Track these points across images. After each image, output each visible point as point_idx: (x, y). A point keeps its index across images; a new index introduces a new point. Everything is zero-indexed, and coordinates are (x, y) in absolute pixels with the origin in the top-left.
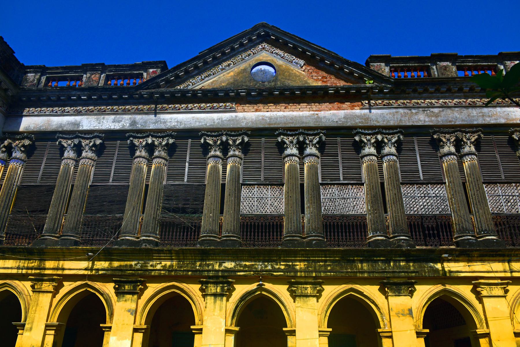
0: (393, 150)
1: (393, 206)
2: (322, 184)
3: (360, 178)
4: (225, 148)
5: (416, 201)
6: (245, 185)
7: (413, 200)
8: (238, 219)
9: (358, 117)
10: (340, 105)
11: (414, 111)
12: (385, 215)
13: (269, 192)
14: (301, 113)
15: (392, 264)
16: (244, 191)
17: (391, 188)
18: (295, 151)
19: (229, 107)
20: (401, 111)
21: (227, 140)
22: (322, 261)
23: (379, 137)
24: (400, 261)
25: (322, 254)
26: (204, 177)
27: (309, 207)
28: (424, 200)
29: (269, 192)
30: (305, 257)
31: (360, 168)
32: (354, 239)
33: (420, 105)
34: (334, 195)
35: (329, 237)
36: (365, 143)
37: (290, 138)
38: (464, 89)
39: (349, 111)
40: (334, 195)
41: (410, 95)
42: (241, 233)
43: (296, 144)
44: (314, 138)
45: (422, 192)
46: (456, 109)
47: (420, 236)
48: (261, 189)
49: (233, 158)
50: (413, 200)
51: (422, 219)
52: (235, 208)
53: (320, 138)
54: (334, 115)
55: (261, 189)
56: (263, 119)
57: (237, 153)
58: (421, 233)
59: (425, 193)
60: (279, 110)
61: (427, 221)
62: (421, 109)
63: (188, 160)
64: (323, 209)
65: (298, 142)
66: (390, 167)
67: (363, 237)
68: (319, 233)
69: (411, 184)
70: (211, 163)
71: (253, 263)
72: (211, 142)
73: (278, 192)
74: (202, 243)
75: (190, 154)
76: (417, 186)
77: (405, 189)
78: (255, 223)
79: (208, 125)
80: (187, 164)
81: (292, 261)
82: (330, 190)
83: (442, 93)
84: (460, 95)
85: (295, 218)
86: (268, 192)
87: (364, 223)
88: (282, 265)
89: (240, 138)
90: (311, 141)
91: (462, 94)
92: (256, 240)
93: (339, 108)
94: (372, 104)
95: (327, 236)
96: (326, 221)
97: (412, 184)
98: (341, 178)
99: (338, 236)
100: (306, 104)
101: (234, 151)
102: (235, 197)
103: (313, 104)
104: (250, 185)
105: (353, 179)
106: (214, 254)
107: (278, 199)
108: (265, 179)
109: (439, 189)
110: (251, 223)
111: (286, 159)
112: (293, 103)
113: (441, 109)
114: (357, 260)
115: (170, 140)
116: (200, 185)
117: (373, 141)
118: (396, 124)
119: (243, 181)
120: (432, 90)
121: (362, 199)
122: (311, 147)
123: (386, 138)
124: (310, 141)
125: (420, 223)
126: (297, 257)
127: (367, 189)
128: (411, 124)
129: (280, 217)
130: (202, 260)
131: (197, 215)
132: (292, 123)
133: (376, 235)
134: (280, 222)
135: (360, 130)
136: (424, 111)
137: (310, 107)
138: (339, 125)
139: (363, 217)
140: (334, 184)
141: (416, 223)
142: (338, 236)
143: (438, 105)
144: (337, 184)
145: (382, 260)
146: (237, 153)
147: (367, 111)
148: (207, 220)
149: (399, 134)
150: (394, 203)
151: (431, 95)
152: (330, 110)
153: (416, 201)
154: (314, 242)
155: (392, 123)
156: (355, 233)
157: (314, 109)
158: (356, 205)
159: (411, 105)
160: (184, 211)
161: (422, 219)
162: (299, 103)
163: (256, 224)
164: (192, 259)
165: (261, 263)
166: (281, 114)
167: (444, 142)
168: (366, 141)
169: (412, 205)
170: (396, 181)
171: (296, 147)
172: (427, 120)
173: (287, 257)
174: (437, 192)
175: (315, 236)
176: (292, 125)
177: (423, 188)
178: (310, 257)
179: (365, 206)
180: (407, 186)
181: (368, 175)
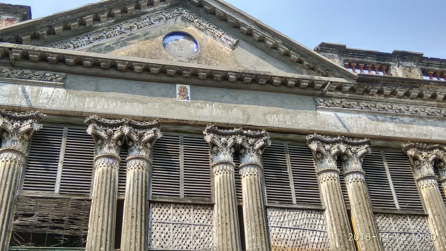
3: (319, 203)
6: (154, 202)
26: (89, 187)
29: (192, 215)
33: (387, 111)
38: (439, 96)
41: (374, 97)
43: (231, 148)
44: (256, 142)
45: (400, 226)
46: (430, 120)
48: (179, 211)
49: (138, 161)
55: (179, 211)
57: (143, 153)
59: (404, 227)
62: (388, 116)
73: (204, 217)
75: (67, 151)
80: (60, 166)
83: (412, 99)
84: (432, 103)
86: (190, 216)
90: (253, 145)
91: (435, 103)
98: (294, 201)
101: (140, 150)
105: (310, 203)
107: (206, 228)
108: (187, 195)
109: (421, 224)
113: (412, 119)
115: (35, 125)
117: (333, 152)
118: (360, 132)
120: (401, 92)
122: (252, 154)
128: (378, 134)
140: (284, 209)
143: (409, 113)
146: (143, 153)
151: (399, 99)
159: (377, 110)
167: (420, 161)
169: (389, 245)
172: (397, 130)
174: (419, 227)
177: (400, 221)
180: (380, 217)
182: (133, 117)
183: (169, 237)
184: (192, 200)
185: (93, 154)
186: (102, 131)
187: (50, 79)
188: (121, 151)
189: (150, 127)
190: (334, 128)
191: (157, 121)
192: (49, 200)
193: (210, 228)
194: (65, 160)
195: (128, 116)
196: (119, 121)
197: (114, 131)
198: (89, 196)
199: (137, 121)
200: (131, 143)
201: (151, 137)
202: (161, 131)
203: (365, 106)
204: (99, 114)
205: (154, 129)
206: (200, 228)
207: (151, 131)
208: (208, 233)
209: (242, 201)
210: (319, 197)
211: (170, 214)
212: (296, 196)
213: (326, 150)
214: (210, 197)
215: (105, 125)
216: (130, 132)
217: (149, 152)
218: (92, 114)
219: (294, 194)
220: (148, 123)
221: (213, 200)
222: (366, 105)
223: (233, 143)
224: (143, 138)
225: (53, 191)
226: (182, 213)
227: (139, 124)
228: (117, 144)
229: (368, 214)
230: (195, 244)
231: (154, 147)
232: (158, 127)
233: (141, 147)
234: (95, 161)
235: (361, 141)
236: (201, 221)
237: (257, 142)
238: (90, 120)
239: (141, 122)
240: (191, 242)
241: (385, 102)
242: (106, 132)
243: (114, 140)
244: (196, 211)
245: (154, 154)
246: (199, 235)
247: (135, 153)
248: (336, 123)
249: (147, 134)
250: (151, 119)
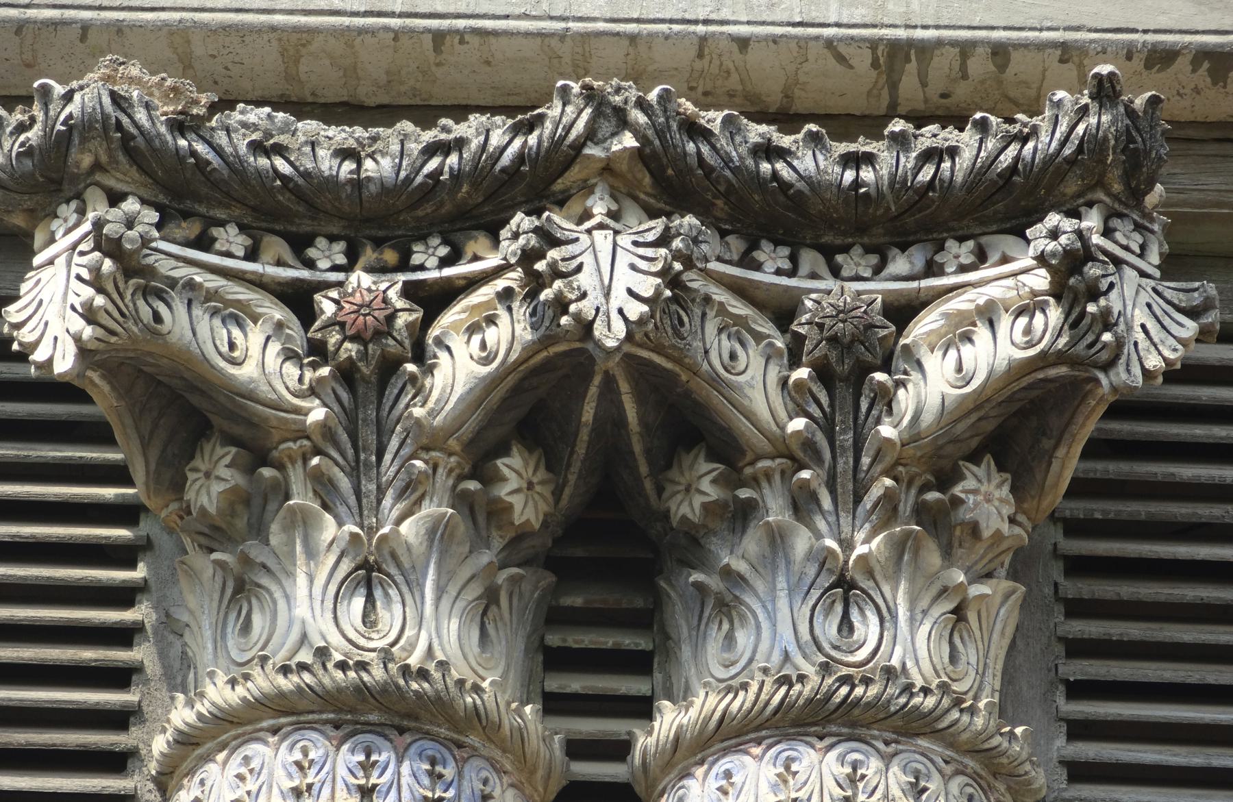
101: (845, 588)
146: (904, 641)
182: (718, 66)
185: (120, 677)
186: (239, 316)
188: (555, 617)
189: (998, 207)
191: (1106, 91)
195: (635, 52)
196: (490, 136)
197: (434, 299)
199: (788, 120)
200: (699, 489)
201: (1019, 370)
202: (1172, 267)
204: (179, 47)
205: (1053, 231)
207: (1017, 272)
215: (292, 213)
216: (676, 298)
217: (1006, 619)
218: (85, 43)
220: (967, 140)
224: (885, 399)
227: (806, 162)
228: (480, 513)
231: (1075, 528)
232: (1127, 204)
233: (869, 545)
238: (60, 144)
239: (843, 124)
242: (307, 314)
243: (427, 441)
245: (1078, 649)
247: (766, 640)
249: (959, 333)
250: (992, 77)
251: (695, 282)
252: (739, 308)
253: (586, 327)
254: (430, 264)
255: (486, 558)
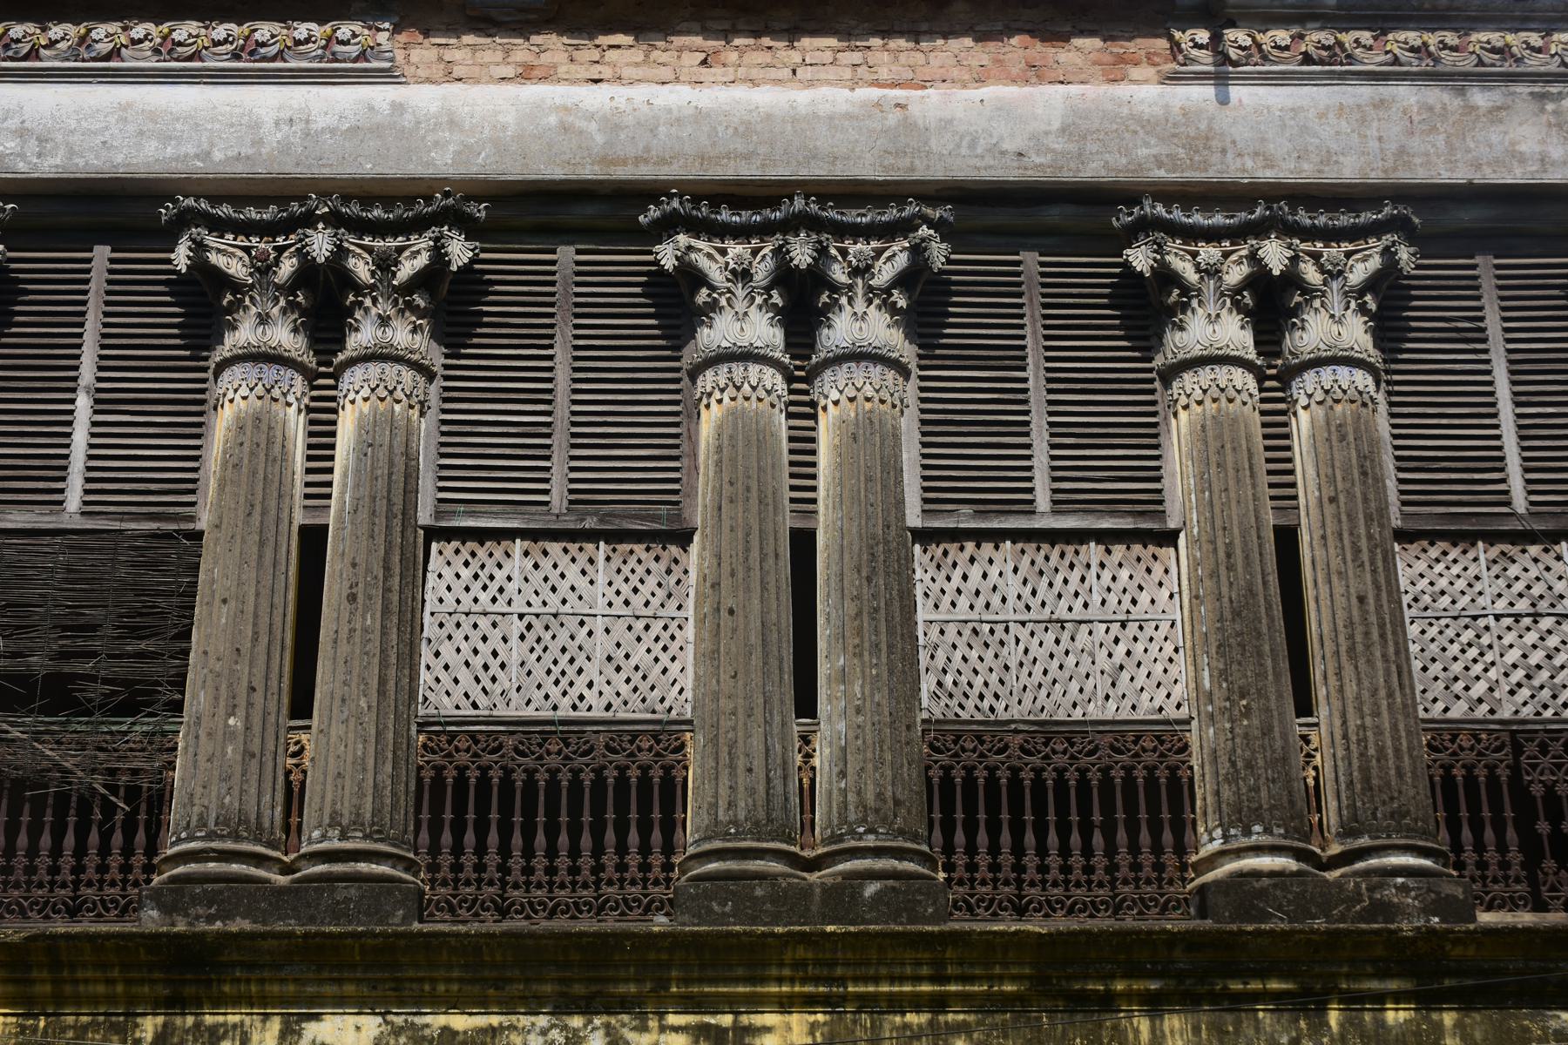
0: (1356, 334)
1: (1348, 671)
2: (925, 536)
4: (325, 304)
5: (1485, 640)
6: (448, 534)
7: (1468, 635)
8: (402, 744)
9: (1149, 125)
10: (1039, 50)
11: (1481, 98)
12: (1297, 726)
13: (601, 580)
14: (802, 98)
15: (1334, 1018)
16: (446, 574)
17: (1335, 563)
18: (763, 331)
19: (353, 50)
20: (1406, 95)
21: (340, 253)
22: (917, 1003)
23: (1275, 254)
24: (1380, 999)
25: (918, 963)
27: (843, 676)
28: (1531, 637)
29: (601, 580)
30: (817, 980)
31: (1151, 437)
32: (1112, 868)
33: (1519, 61)
34: (996, 600)
35: (960, 860)
36: (1186, 289)
37: (736, 249)
39: (1096, 93)
40: (996, 600)
42: (424, 836)
43: (768, 290)
44: (879, 253)
45: (1519, 587)
47: (1502, 848)
48: (546, 564)
49: (374, 369)
50: (1468, 635)
51: (1518, 749)
52: (382, 681)
53: (917, 251)
54: (1003, 109)
55: (546, 564)
56: (565, 128)
57: (401, 335)
58: (1511, 834)
59: (1537, 590)
60: (666, 73)
61: (1546, 761)
62: (1523, 89)
63: (87, 372)
64: (927, 684)
65: (785, 276)
66: (1334, 434)
67: (1169, 858)
68: (901, 832)
69: (1455, 538)
70: (234, 399)
71: (495, 1020)
72: (237, 268)
73: (651, 581)
74: (175, 897)
76: (1494, 552)
77: (1421, 566)
78: (508, 772)
79: (218, 156)
80: (83, 403)
81: (732, 1004)
82: (975, 573)
85: (757, 743)
86: (593, 581)
87: (1173, 770)
88: (676, 1029)
89: (422, 243)
92: (516, 875)
93: (1035, 73)
94: (1233, 54)
95: (948, 849)
96: (944, 759)
97: (1464, 539)
98: (1043, 500)
99: (1018, 850)
100: (832, 42)
101: (384, 321)
102: (386, 611)
103: (876, 42)
104: (481, 535)
105: (1111, 505)
106: (251, 966)
107: (657, 627)
108: (577, 501)
110: (484, 770)
111: (708, 379)
112: (757, 34)
114: (1129, 996)
116: (168, 536)
117: (1235, 274)
118: (1375, 176)
119: (438, 515)
121: (1165, 627)
123: (1316, 256)
124: (855, 272)
125: (1503, 773)
126: (763, 980)
127: (1194, 564)
128: (1460, 175)
129: (666, 735)
130: (174, 1003)
131: (142, 725)
132: (747, 157)
133: (1245, 842)
134: (667, 769)
135: (1160, 209)
136: (1542, 97)
137: (856, 57)
138: (1032, 175)
139: (1166, 737)
140: (997, 536)
141: (1481, 773)
142: (1018, 850)
144: (1016, 535)
145: (1277, 996)
146: (401, 335)
147: (1207, 92)
148: (209, 756)
149: (1388, 239)
150: (1351, 650)
152: (980, 81)
153: (1485, 640)
154: (871, 889)
155: (1349, 170)
156: (1122, 836)
157: (884, 74)
158: (1130, 665)
160: (58, 696)
161: (1518, 749)
162: (792, 33)
163: (519, 778)
164: (111, 1000)
165: (542, 1021)
166: (678, 97)
168: (1191, 276)
169: (1457, 668)
170: (1369, 518)
171: (767, 305)
173: (701, 981)
175: (877, 852)
176: (748, 170)
177: (1527, 564)
178: (842, 981)
179: (1181, 667)
180: (1434, 552)
181: (1204, 484)
183: (503, 666)
184: (601, 521)
187: (25, 48)
190: (1249, 164)
192: (47, 540)
193: (673, 626)
194: (99, 380)
198: (192, 519)
203: (1412, 49)
206: (630, 628)
208: (665, 649)
209: (815, 512)
210: (1158, 479)
211: (509, 579)
212: (1055, 479)
213: (1198, 270)
214: (677, 503)
219: (1046, 470)
221: (686, 515)
222: (1418, 43)
223: (777, 268)
224: (394, 274)
225: (61, 503)
226: (558, 571)
228: (292, 306)
229: (1364, 544)
230: (606, 689)
234: (217, 375)
235: (1367, 217)
236: (638, 601)
237: (886, 254)
240: (590, 685)
241: (1513, 19)
244: (617, 561)
246: (627, 656)
248: (1263, 140)
251: (346, 245)
252: (358, 251)
253: (314, 259)
254: (280, 241)
255: (296, 316)
